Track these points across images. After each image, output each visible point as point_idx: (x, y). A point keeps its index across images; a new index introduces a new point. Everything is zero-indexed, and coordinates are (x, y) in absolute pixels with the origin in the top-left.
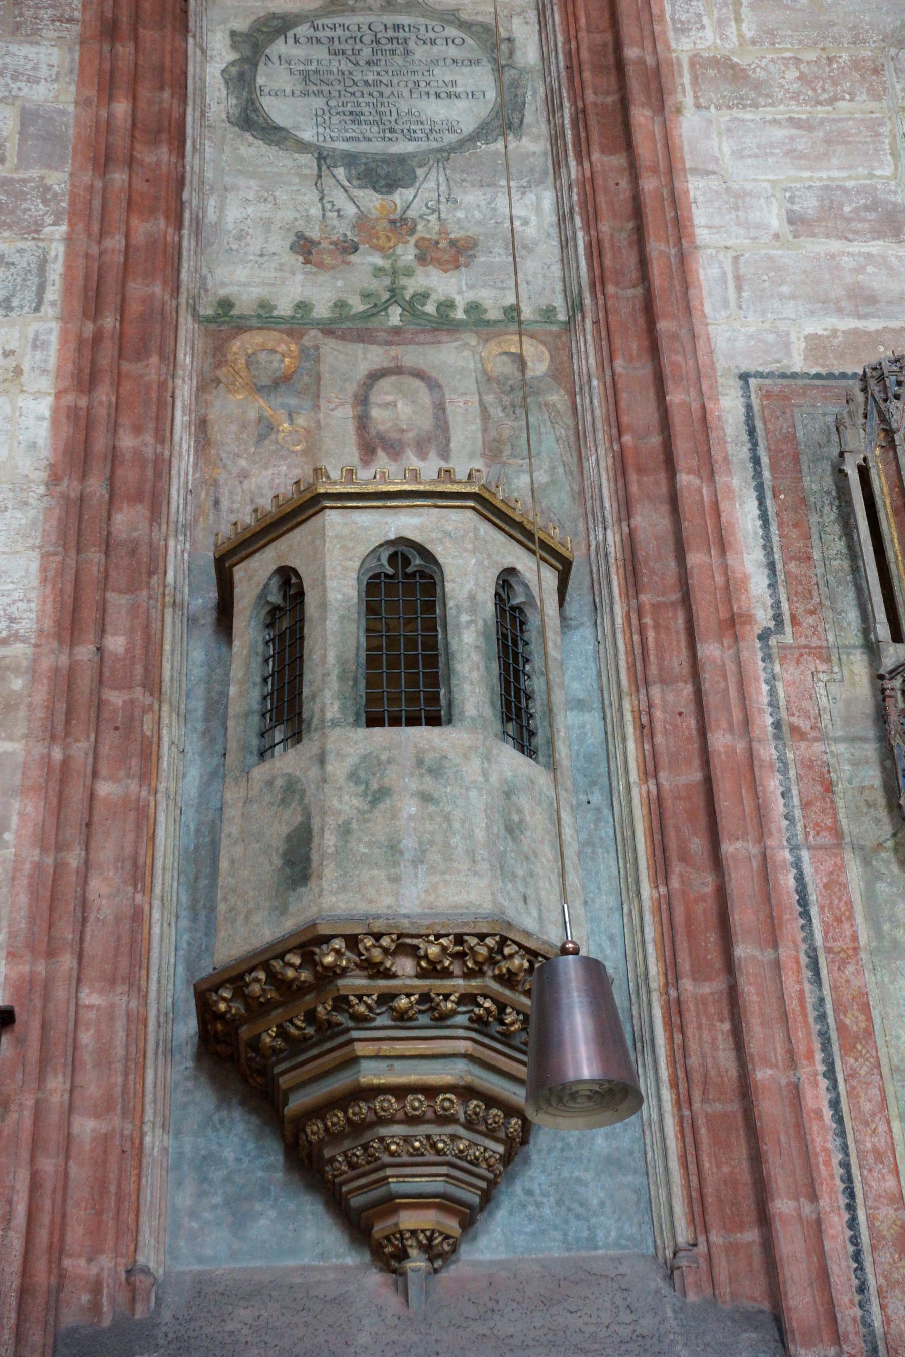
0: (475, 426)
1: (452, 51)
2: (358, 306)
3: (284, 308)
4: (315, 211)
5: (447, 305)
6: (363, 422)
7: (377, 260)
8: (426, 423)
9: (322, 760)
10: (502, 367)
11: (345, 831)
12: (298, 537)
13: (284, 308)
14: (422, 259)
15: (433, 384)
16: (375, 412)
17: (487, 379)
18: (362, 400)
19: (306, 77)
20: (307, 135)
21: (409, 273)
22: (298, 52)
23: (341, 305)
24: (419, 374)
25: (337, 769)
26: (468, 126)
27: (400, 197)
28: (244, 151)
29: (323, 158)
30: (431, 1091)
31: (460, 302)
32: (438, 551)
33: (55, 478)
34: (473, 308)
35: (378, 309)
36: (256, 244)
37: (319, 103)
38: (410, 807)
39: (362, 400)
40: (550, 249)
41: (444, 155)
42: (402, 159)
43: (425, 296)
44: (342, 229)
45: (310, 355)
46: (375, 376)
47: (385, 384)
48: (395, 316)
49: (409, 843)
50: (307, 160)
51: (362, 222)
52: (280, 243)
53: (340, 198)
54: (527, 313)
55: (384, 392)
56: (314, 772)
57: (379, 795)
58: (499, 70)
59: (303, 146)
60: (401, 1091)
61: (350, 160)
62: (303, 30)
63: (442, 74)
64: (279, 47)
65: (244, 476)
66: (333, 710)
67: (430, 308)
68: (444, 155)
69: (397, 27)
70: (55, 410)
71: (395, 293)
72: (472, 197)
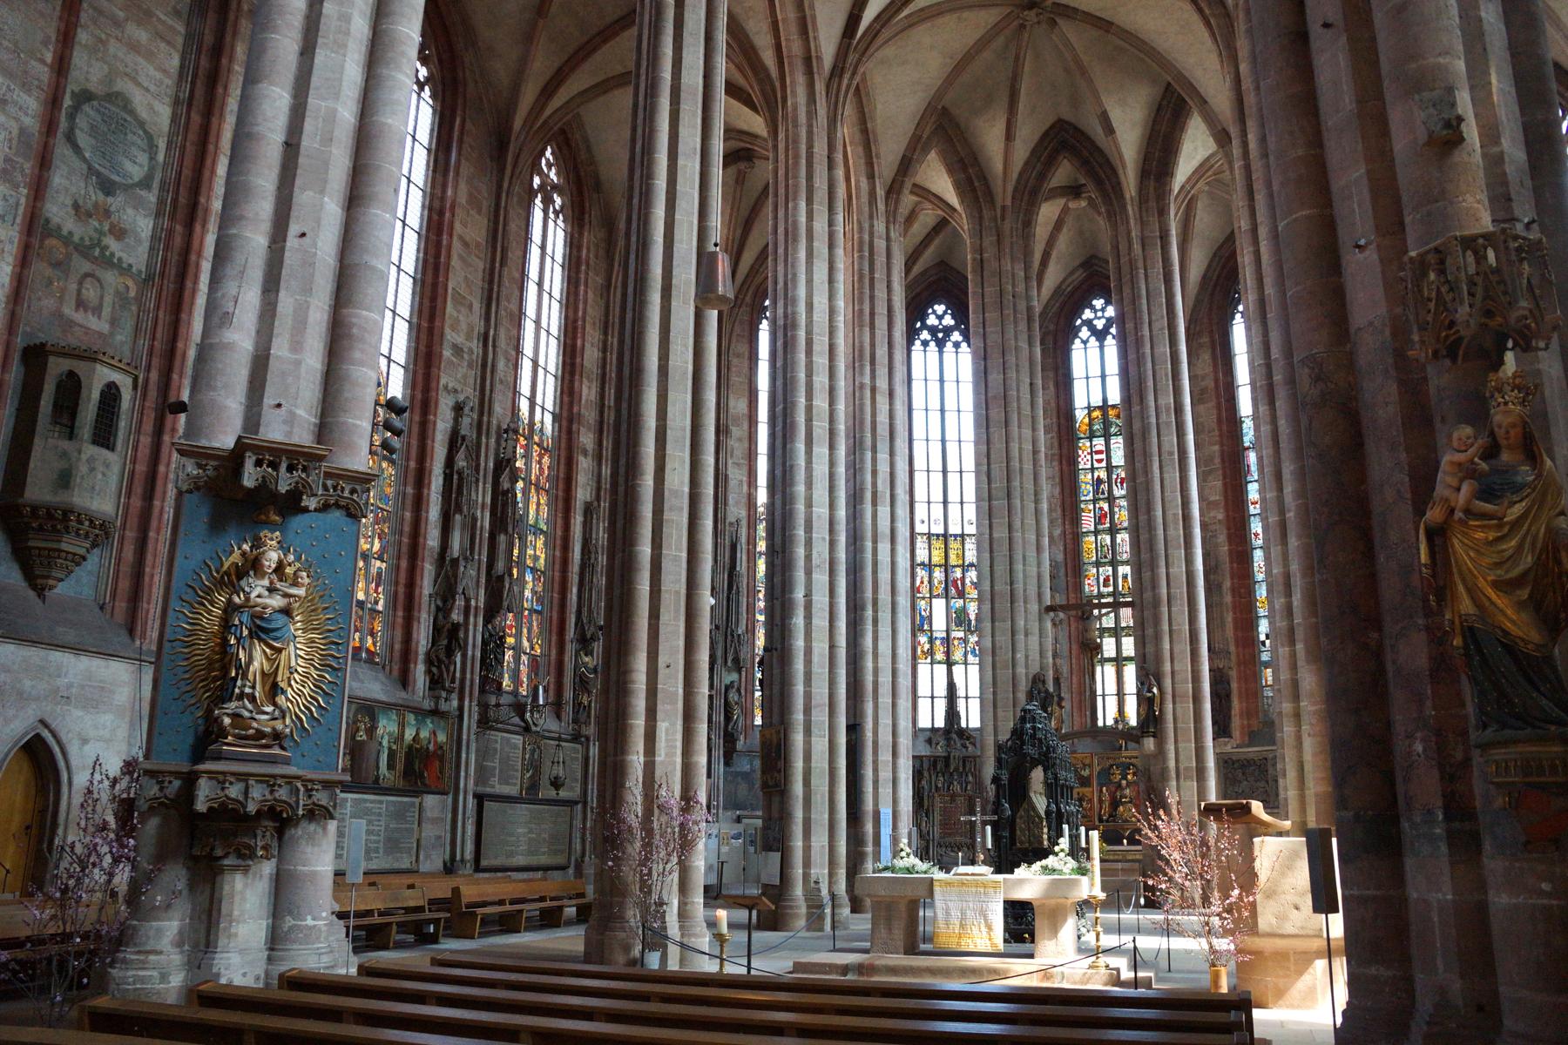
1: (139, 142)
2: (87, 243)
4: (83, 192)
5: (112, 255)
6: (79, 292)
7: (96, 224)
9: (80, 452)
10: (121, 288)
11: (82, 477)
12: (82, 364)
13: (65, 232)
14: (110, 231)
15: (102, 287)
16: (83, 291)
17: (117, 292)
18: (80, 283)
19: (92, 127)
20: (87, 155)
21: (105, 235)
23: (82, 239)
24: (99, 281)
25: (84, 457)
26: (136, 179)
27: (110, 200)
28: (66, 152)
29: (90, 168)
30: (75, 554)
31: (117, 255)
32: (122, 390)
33: (7, 303)
34: (120, 259)
35: (92, 247)
36: (61, 199)
37: (94, 142)
38: (100, 476)
39: (80, 283)
40: (146, 245)
41: (127, 188)
42: (113, 183)
44: (89, 206)
45: (68, 256)
46: (87, 275)
47: (89, 279)
48: (97, 252)
49: (97, 488)
50: (85, 166)
51: (96, 205)
52: (69, 202)
53: (91, 189)
54: (134, 270)
55: (88, 283)
56: (76, 454)
57: (92, 470)
58: (151, 159)
59: (84, 160)
60: (68, 553)
61: (98, 175)
62: (95, 103)
63: (134, 150)
64: (86, 108)
65: (39, 299)
66: (86, 437)
68: (127, 188)
69: (125, 120)
70: (13, 272)
71: (100, 241)
72: (130, 211)
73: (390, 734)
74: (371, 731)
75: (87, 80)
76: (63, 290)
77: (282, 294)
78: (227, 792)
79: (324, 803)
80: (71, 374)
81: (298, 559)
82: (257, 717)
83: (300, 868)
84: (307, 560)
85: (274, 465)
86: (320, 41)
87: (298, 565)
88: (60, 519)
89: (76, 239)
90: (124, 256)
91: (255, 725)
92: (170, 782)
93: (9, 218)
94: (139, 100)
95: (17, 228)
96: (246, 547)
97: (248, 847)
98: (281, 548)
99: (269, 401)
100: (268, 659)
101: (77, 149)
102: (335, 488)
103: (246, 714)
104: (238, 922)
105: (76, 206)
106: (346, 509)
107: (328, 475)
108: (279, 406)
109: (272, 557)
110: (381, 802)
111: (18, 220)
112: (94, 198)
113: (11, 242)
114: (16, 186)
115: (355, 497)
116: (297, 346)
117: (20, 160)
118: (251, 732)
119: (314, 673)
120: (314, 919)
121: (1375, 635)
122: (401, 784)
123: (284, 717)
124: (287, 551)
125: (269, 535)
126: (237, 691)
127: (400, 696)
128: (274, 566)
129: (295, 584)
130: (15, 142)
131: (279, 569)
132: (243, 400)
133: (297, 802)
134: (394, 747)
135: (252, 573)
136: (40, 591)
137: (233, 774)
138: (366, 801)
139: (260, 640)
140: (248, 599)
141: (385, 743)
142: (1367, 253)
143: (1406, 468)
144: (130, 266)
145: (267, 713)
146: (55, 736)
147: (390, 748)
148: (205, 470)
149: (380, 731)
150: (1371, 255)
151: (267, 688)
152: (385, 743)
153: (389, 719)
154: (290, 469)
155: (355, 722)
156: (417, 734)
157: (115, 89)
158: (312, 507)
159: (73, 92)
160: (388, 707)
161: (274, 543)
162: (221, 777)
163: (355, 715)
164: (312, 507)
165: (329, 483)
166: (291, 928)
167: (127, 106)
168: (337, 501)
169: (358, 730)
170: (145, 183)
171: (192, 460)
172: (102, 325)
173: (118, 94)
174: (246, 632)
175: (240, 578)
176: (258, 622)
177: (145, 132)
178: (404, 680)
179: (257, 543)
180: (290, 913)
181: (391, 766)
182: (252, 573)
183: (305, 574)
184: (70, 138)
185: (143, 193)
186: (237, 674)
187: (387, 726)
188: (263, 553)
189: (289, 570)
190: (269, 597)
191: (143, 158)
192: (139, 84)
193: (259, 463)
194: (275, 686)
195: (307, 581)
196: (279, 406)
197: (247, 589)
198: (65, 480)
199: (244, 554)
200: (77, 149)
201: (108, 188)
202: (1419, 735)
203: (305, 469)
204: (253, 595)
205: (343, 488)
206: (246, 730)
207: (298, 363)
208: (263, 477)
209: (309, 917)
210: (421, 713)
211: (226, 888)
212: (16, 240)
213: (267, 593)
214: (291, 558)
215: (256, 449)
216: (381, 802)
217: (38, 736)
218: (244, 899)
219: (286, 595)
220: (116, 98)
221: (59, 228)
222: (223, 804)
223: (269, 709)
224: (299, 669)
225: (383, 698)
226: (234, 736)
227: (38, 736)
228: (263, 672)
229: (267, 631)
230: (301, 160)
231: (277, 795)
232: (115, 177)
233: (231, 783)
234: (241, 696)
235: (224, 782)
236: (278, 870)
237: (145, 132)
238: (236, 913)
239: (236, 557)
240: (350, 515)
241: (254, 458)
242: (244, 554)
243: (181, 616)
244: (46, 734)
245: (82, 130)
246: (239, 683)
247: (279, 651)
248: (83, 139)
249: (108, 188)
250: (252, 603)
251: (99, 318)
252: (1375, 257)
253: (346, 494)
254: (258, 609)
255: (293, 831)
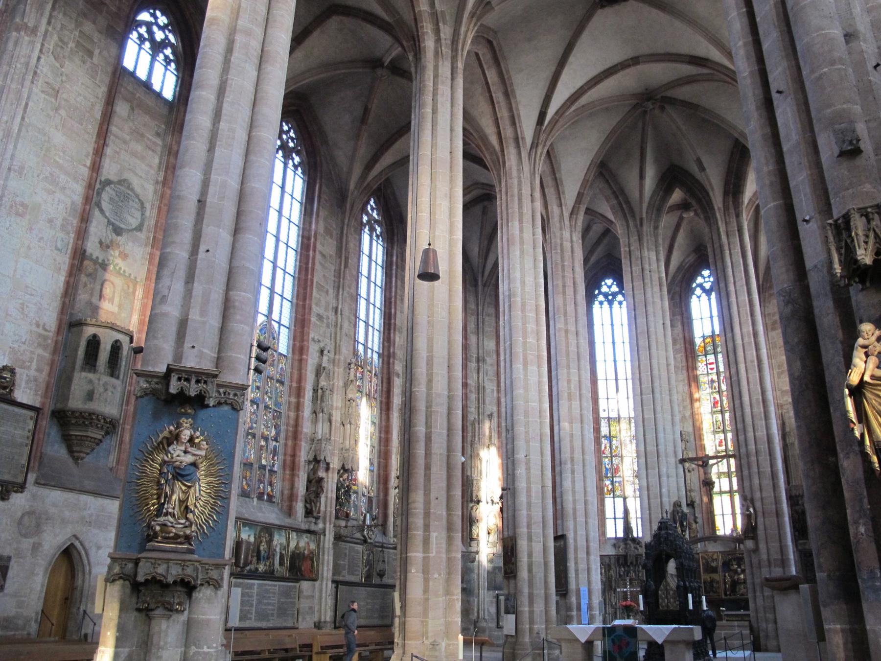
0: (118, 299)
1: (136, 205)
3: (94, 257)
4: (104, 235)
5: (120, 268)
8: (111, 296)
9: (99, 380)
13: (94, 257)
15: (114, 287)
19: (111, 199)
20: (107, 214)
22: (111, 192)
25: (101, 383)
26: (134, 226)
27: (119, 238)
33: (61, 298)
34: (124, 271)
37: (111, 206)
42: (122, 229)
43: (117, 264)
44: (108, 242)
45: (96, 270)
50: (106, 221)
52: (97, 241)
53: (109, 232)
58: (142, 215)
59: (106, 217)
61: (113, 225)
62: (112, 186)
63: (133, 211)
64: (107, 189)
67: (118, 268)
73: (281, 544)
74: (270, 542)
75: (108, 173)
76: (92, 290)
77: (196, 284)
78: (156, 570)
79: (215, 577)
80: (95, 336)
81: (202, 434)
82: (176, 526)
83: (201, 617)
84: (208, 435)
85: (188, 380)
86: (218, 143)
87: (202, 438)
88: (89, 418)
89: (100, 261)
90: (127, 269)
91: (174, 530)
92: (126, 564)
93: (64, 250)
94: (136, 183)
95: (68, 256)
96: (172, 428)
97: (169, 603)
98: (193, 428)
99: (187, 345)
100: (183, 492)
101: (102, 211)
102: (225, 393)
103: (170, 524)
104: (163, 649)
105: (101, 243)
106: (231, 404)
107: (220, 386)
108: (193, 347)
109: (186, 434)
110: (275, 586)
111: (69, 251)
112: (110, 238)
113: (64, 263)
114: (68, 233)
115: (236, 398)
116: (203, 313)
117: (71, 218)
118: (172, 535)
119: (212, 501)
120: (208, 648)
121: (834, 459)
122: (287, 574)
123: (191, 526)
124: (195, 430)
125: (185, 421)
126: (164, 511)
127: (287, 521)
128: (188, 438)
129: (200, 449)
130: (69, 209)
131: (191, 440)
132: (173, 344)
133: (197, 576)
134: (284, 552)
135: (175, 442)
136: (76, 460)
137: (160, 559)
138: (266, 585)
139: (178, 480)
140: (172, 458)
141: (278, 550)
142: (811, 224)
143: (842, 353)
144: (130, 274)
145: (181, 524)
146: (82, 544)
147: (281, 553)
148: (150, 384)
149: (275, 543)
150: (813, 226)
151: (182, 508)
152: (278, 550)
153: (280, 535)
154: (198, 382)
155: (260, 537)
156: (298, 544)
157: (123, 178)
158: (211, 405)
159: (101, 181)
160: (280, 528)
161: (188, 425)
162: (153, 561)
163: (260, 532)
164: (211, 405)
165: (222, 390)
166: (195, 653)
167: (129, 186)
168: (226, 401)
169: (261, 542)
170: (139, 228)
171: (144, 379)
172: (115, 309)
173: (125, 180)
174: (170, 476)
175: (169, 445)
176: (178, 471)
177: (140, 200)
178: (290, 512)
179: (179, 425)
180: (195, 644)
181: (281, 563)
182: (175, 442)
183: (205, 443)
184: (98, 205)
185: (138, 234)
186: (165, 501)
187: (279, 540)
188: (182, 431)
189: (197, 441)
190: (184, 456)
191: (138, 214)
192: (136, 174)
193: (179, 379)
194: (187, 507)
195: (206, 447)
196: (193, 347)
197: (172, 452)
198: (90, 396)
199: (170, 432)
200: (102, 211)
201: (118, 231)
202: (861, 521)
203: (205, 382)
204: (175, 455)
205: (229, 394)
206: (169, 534)
207: (204, 323)
208: (182, 388)
209: (205, 647)
210: (299, 531)
211: (157, 628)
212: (67, 263)
213: (183, 454)
214: (198, 434)
215: (178, 371)
216: (275, 586)
217: (72, 544)
218: (167, 635)
219: (194, 455)
220: (124, 181)
221: (91, 255)
222: (154, 578)
223: (183, 521)
224: (202, 498)
225: (277, 522)
226: (162, 537)
227: (72, 544)
228: (179, 498)
229: (183, 476)
230: (207, 209)
231: (185, 572)
232: (122, 226)
233: (159, 565)
234: (166, 514)
235: (155, 564)
236: (188, 618)
237: (140, 200)
238: (162, 643)
239: (166, 433)
240: (234, 409)
241: (177, 376)
242: (170, 432)
243: (135, 468)
244: (77, 544)
245: (104, 201)
246: (166, 506)
247: (189, 487)
248: (105, 205)
249: (118, 231)
250: (174, 460)
251: (112, 304)
252: (815, 226)
253: (231, 396)
254: (178, 463)
255: (197, 595)
